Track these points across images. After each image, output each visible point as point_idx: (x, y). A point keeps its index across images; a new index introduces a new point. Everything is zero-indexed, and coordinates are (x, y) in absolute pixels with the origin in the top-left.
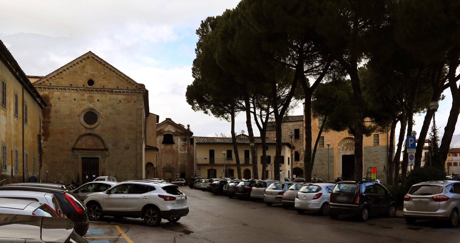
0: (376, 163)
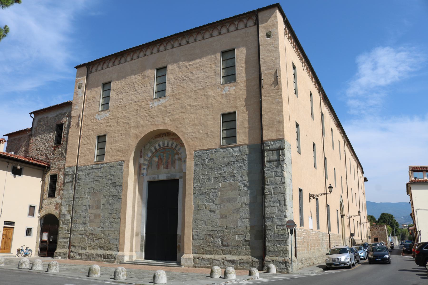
0: (228, 200)
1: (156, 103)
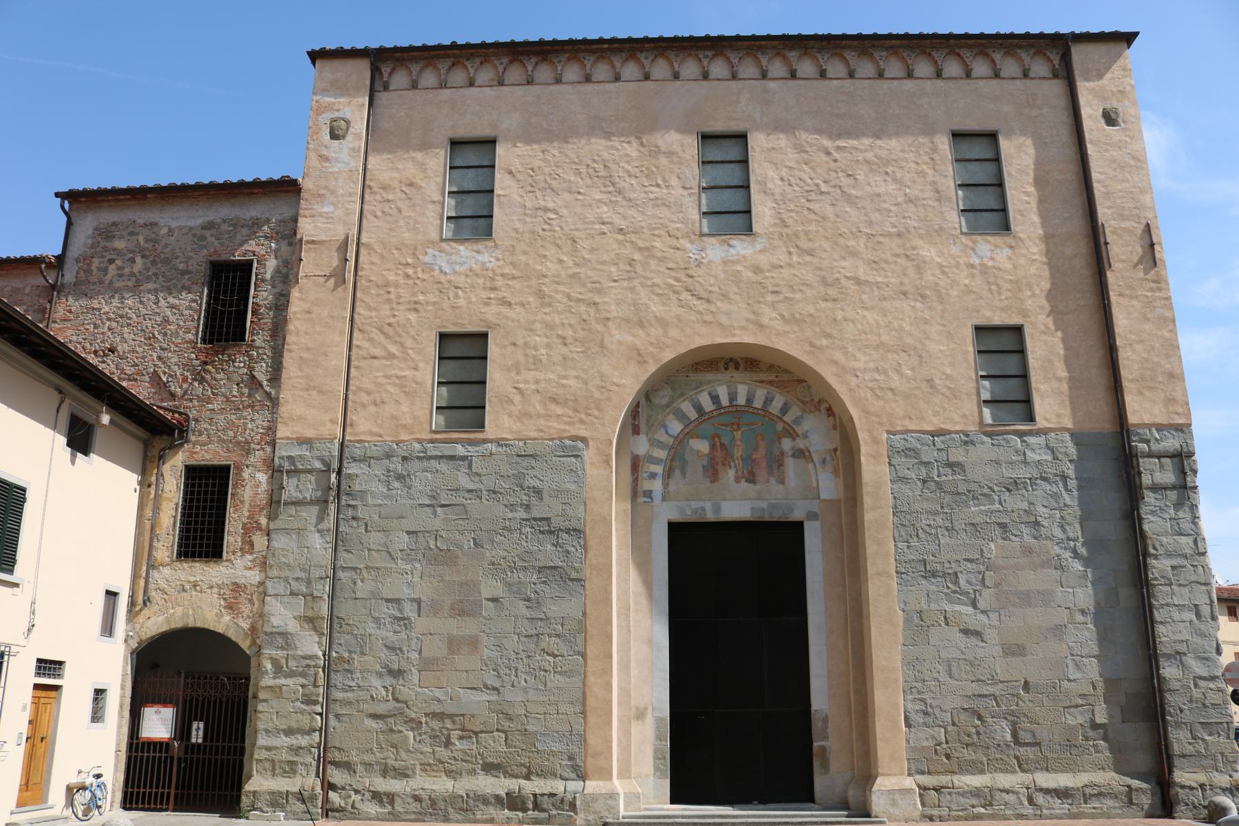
0: (1026, 599)
1: (715, 251)
